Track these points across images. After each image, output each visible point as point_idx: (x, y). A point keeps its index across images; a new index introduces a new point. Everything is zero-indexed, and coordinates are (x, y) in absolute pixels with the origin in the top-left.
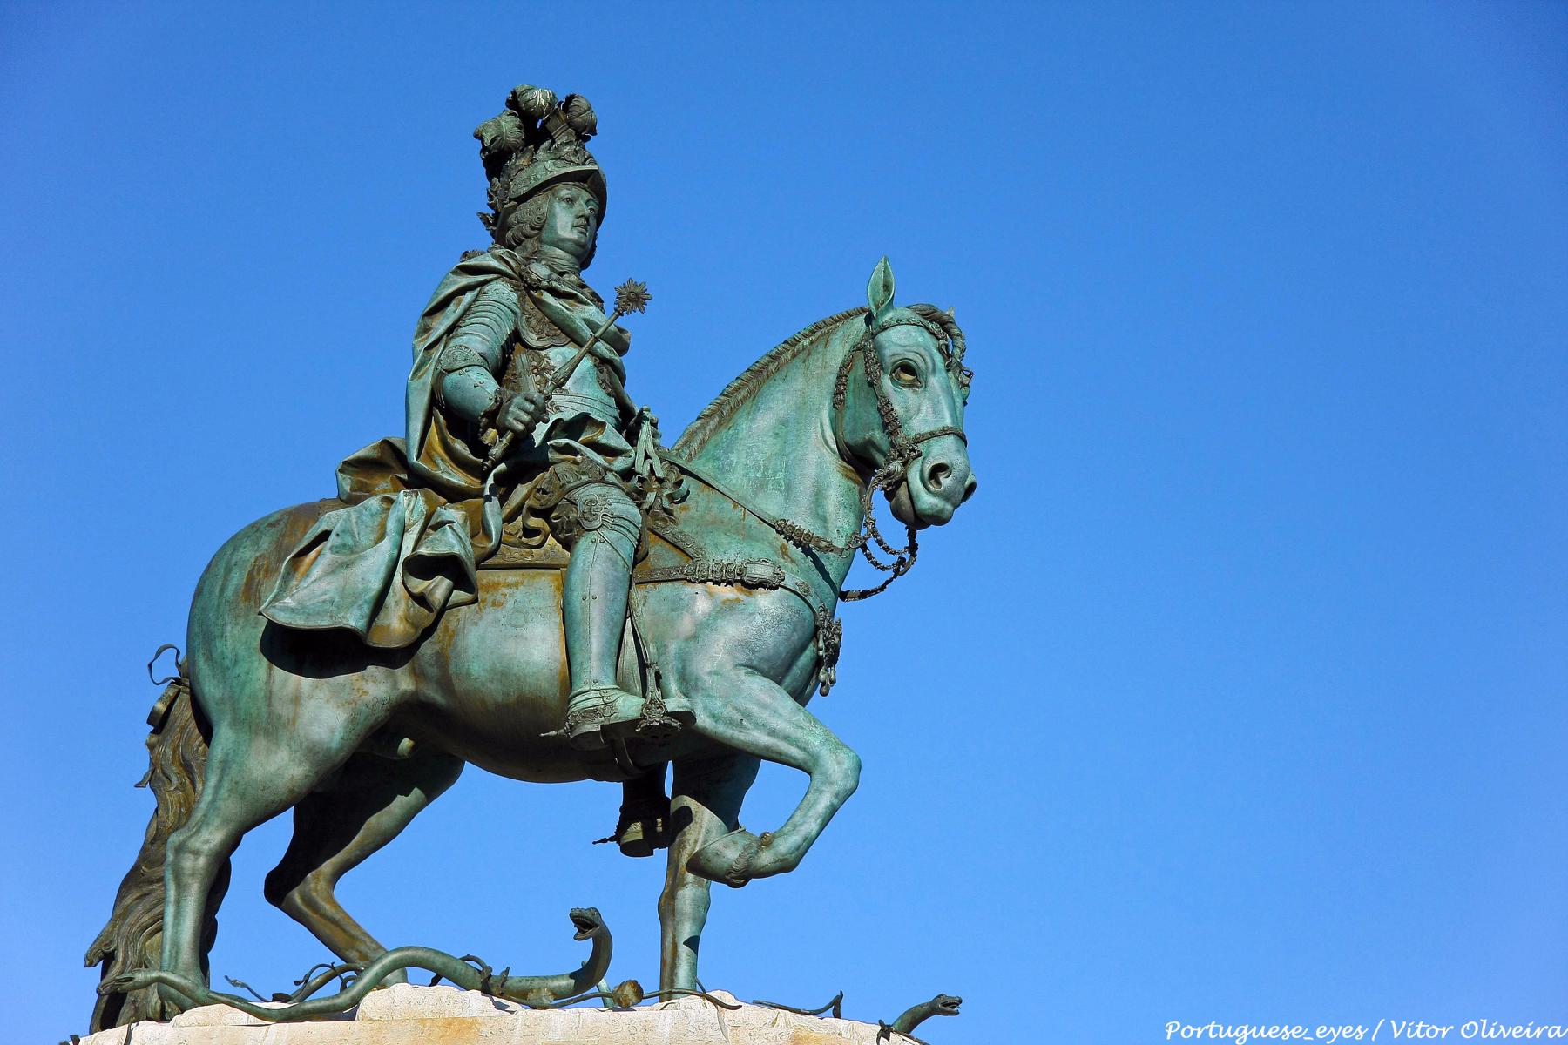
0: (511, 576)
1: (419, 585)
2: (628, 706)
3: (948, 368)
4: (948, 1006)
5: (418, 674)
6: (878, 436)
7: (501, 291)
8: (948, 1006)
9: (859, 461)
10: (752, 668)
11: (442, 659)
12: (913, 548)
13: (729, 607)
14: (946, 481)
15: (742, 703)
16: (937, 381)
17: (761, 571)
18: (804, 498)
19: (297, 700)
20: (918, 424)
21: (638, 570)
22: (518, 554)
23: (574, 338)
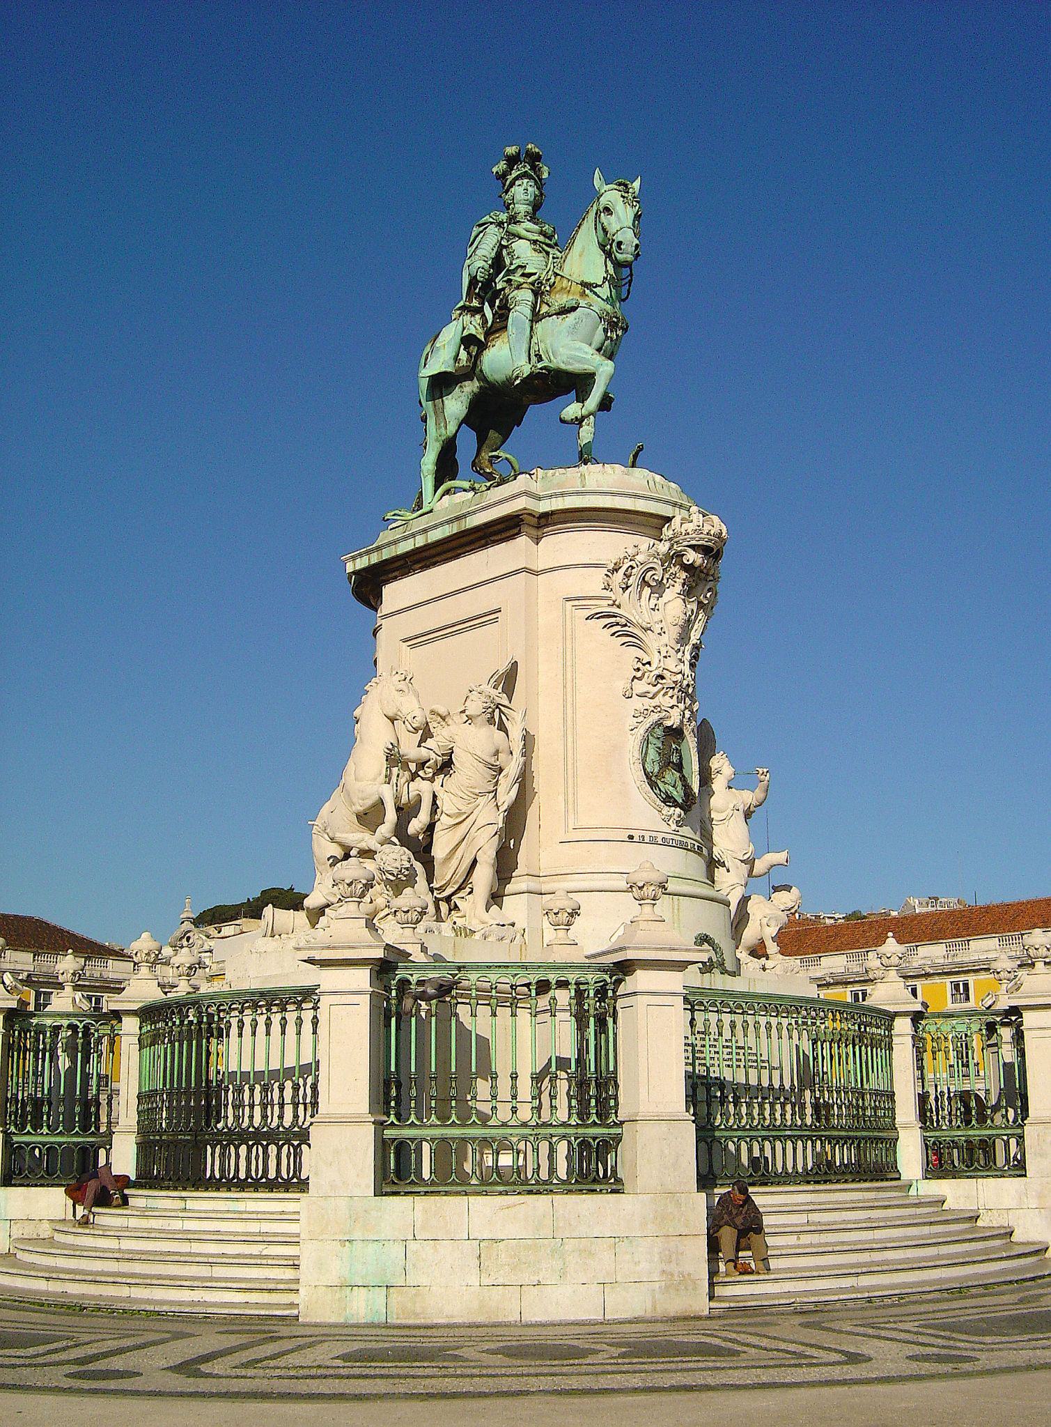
2: (526, 371)
8: (640, 449)
12: (631, 275)
21: (536, 317)
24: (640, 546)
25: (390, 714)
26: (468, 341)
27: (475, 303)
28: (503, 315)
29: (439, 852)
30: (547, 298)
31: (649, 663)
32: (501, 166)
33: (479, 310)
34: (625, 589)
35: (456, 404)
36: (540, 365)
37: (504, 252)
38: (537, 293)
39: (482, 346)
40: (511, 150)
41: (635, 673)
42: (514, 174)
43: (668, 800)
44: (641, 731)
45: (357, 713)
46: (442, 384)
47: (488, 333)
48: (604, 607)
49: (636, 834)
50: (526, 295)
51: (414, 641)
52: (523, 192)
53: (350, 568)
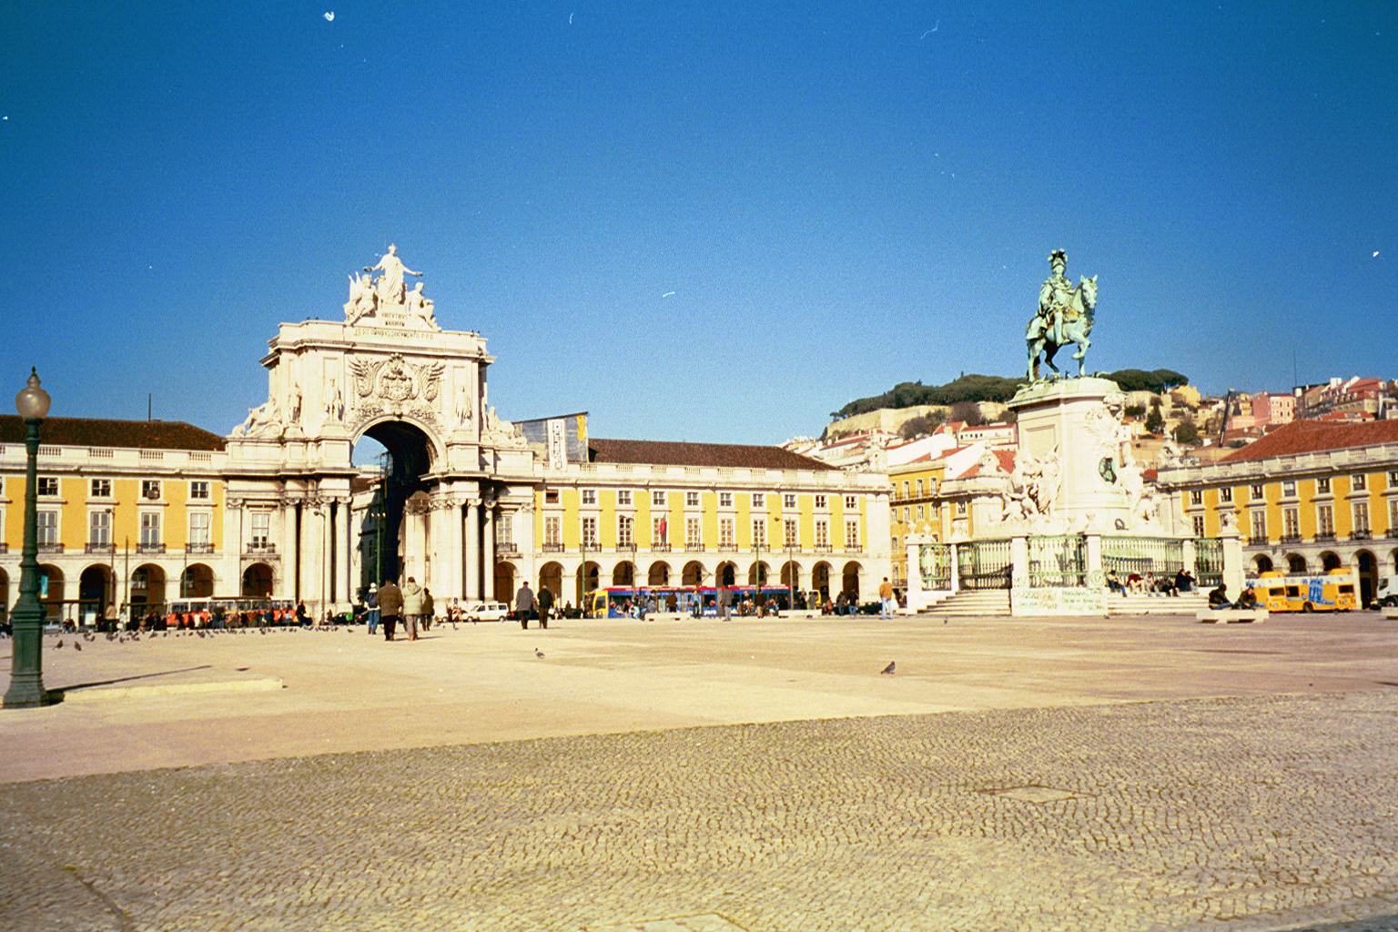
21: (1064, 322)
24: (1100, 403)
26: (1042, 328)
28: (1053, 319)
29: (1039, 498)
32: (1051, 258)
35: (1039, 346)
38: (1064, 312)
39: (1046, 330)
40: (1054, 252)
43: (1107, 480)
44: (1098, 462)
46: (1032, 342)
47: (1048, 325)
51: (1030, 430)
52: (1059, 269)
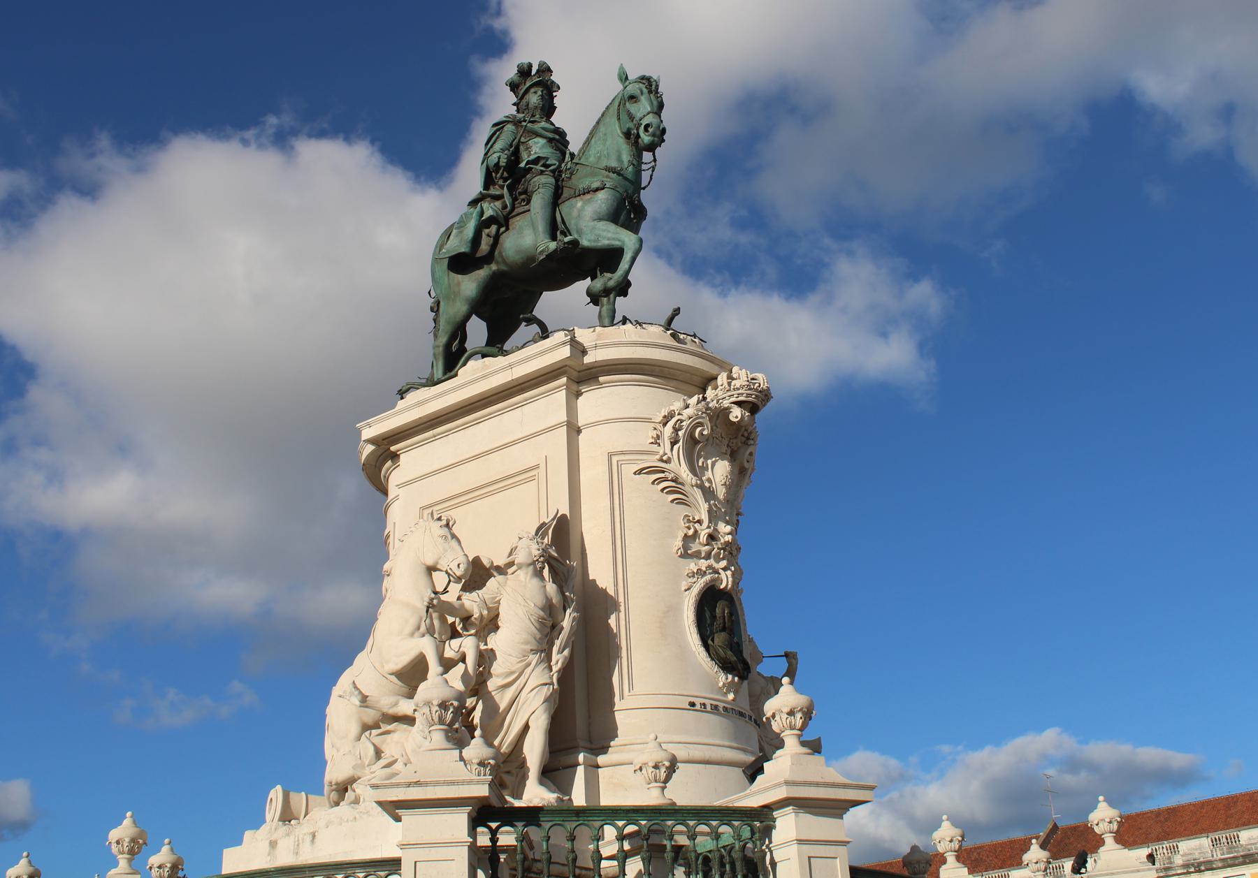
0: (518, 218)
1: (487, 231)
2: (553, 245)
3: (650, 92)
4: (677, 312)
5: (497, 263)
6: (631, 125)
7: (510, 127)
8: (677, 312)
9: (627, 135)
10: (600, 219)
11: (500, 253)
12: (655, 160)
13: (589, 201)
14: (651, 130)
15: (597, 232)
16: (643, 99)
17: (596, 185)
18: (614, 157)
19: (459, 284)
20: (639, 115)
21: (556, 199)
22: (521, 209)
23: (538, 135)
25: (430, 562)
27: (494, 191)
30: (569, 183)
31: (700, 522)
33: (499, 197)
34: (673, 444)
36: (566, 239)
37: (522, 148)
41: (685, 531)
42: (528, 84)
43: (726, 666)
44: (696, 590)
45: (386, 567)
48: (652, 461)
49: (698, 701)
50: (547, 179)
53: (367, 433)
